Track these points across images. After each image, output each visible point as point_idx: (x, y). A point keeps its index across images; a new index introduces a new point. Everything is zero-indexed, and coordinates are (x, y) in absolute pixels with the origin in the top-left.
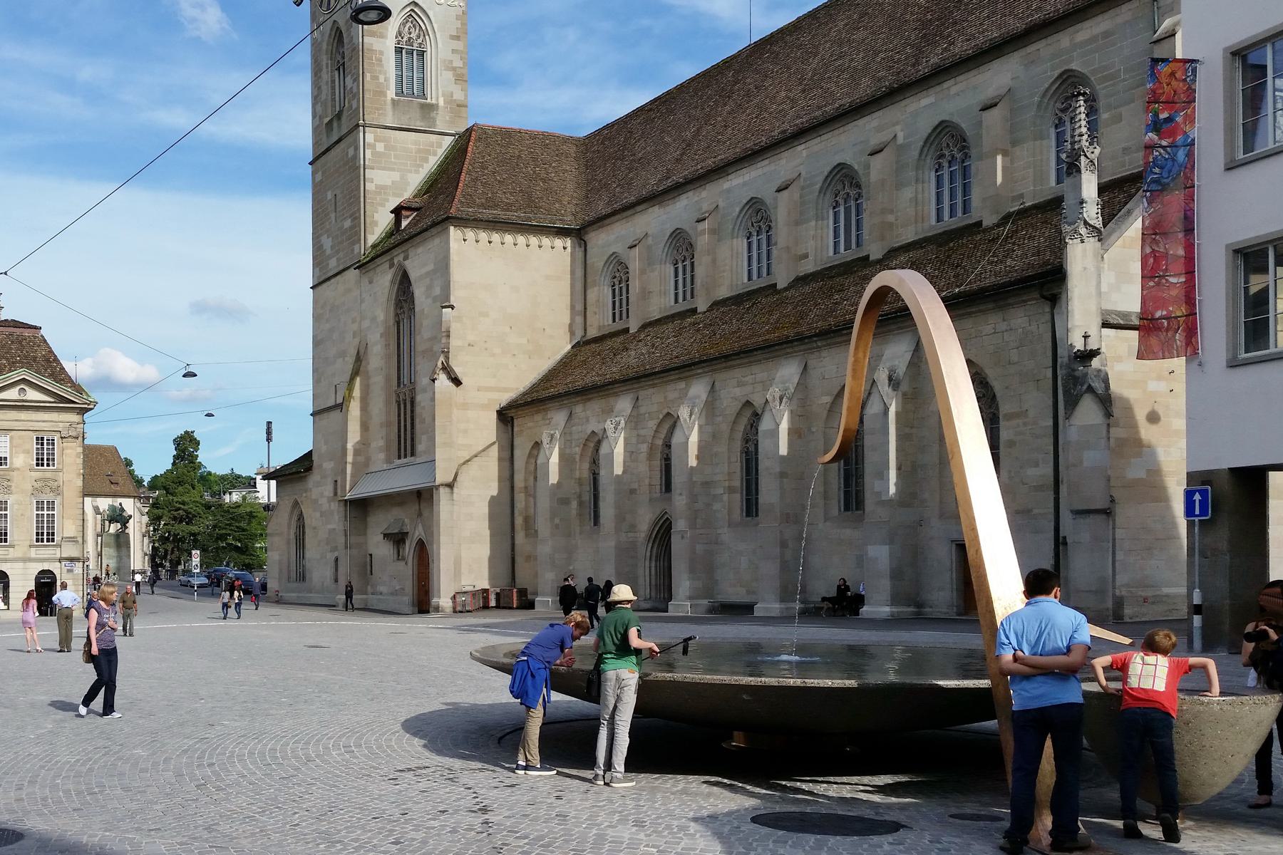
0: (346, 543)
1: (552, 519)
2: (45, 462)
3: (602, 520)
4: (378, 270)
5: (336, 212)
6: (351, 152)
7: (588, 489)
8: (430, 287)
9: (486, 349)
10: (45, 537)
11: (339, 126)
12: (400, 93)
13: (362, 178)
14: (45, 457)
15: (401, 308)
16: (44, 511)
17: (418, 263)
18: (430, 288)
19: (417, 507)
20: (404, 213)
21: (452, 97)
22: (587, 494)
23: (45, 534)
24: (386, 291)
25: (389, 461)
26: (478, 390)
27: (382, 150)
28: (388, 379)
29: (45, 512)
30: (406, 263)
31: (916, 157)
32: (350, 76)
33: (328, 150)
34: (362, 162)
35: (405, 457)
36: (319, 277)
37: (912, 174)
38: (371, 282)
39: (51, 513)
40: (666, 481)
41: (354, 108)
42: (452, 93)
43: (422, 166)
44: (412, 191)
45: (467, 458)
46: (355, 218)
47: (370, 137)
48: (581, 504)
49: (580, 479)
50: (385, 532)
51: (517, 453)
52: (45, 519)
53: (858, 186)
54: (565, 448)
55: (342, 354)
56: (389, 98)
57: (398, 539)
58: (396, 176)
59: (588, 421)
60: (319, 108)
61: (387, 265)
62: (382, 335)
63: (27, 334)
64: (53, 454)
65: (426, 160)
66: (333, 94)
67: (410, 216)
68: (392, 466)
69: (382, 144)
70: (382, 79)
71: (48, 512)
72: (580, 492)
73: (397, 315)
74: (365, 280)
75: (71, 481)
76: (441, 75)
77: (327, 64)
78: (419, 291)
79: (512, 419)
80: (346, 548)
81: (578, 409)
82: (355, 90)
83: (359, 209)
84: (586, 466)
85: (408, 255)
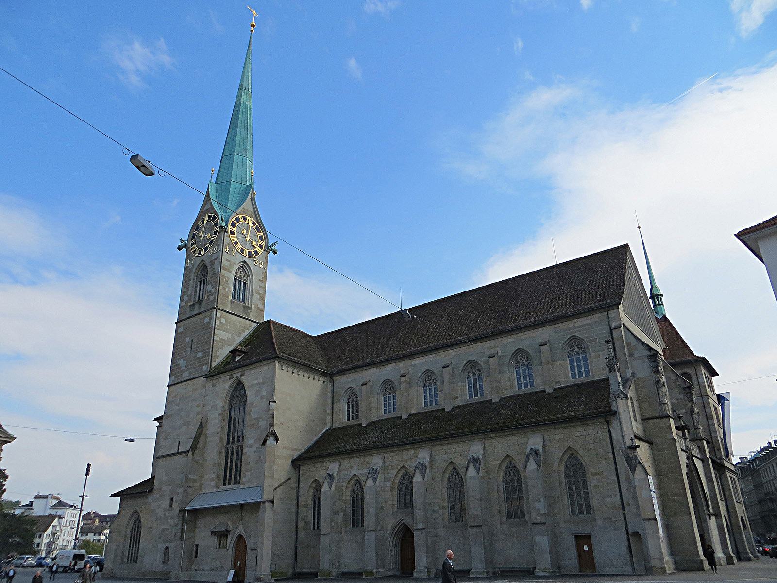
11: (199, 307)
12: (234, 297)
17: (251, 378)
19: (240, 515)
28: (221, 440)
35: (230, 484)
38: (214, 386)
45: (277, 486)
46: (206, 352)
48: (345, 514)
51: (301, 485)
57: (222, 535)
58: (229, 336)
60: (185, 298)
66: (196, 292)
68: (219, 490)
69: (224, 319)
74: (209, 385)
83: (209, 349)
85: (244, 374)
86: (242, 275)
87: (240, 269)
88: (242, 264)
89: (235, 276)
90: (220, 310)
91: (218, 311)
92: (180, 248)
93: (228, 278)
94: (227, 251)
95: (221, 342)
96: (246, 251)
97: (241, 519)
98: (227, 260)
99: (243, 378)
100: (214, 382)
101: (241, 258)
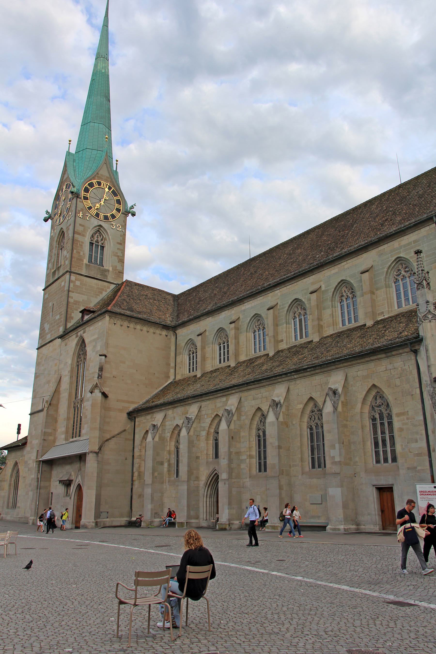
0: (38, 486)
1: (153, 474)
3: (180, 474)
4: (70, 339)
5: (53, 312)
6: (63, 284)
7: (174, 456)
8: (95, 347)
9: (123, 380)
11: (58, 273)
12: (90, 261)
15: (80, 358)
18: (95, 347)
20: (85, 312)
22: (173, 459)
25: (66, 439)
26: (117, 401)
28: (70, 395)
30: (84, 334)
31: (331, 296)
32: (66, 251)
33: (53, 283)
36: (41, 344)
37: (330, 303)
38: (66, 345)
40: (215, 451)
42: (116, 266)
43: (99, 295)
46: (62, 315)
48: (169, 465)
49: (169, 451)
50: (60, 480)
51: (136, 436)
53: (305, 309)
54: (162, 433)
55: (49, 382)
58: (85, 298)
59: (174, 418)
61: (75, 336)
62: (69, 372)
65: (101, 293)
69: (79, 282)
70: (82, 254)
72: (170, 459)
73: (78, 362)
74: (63, 344)
77: (56, 247)
78: (89, 349)
80: (37, 488)
81: (170, 412)
84: (173, 443)
86: (99, 239)
88: (98, 228)
89: (92, 240)
90: (74, 273)
91: (72, 274)
92: (46, 220)
93: (83, 243)
94: (81, 216)
95: (76, 304)
96: (102, 215)
97: (80, 470)
98: (80, 225)
99: (85, 336)
100: (67, 341)
101: (95, 222)
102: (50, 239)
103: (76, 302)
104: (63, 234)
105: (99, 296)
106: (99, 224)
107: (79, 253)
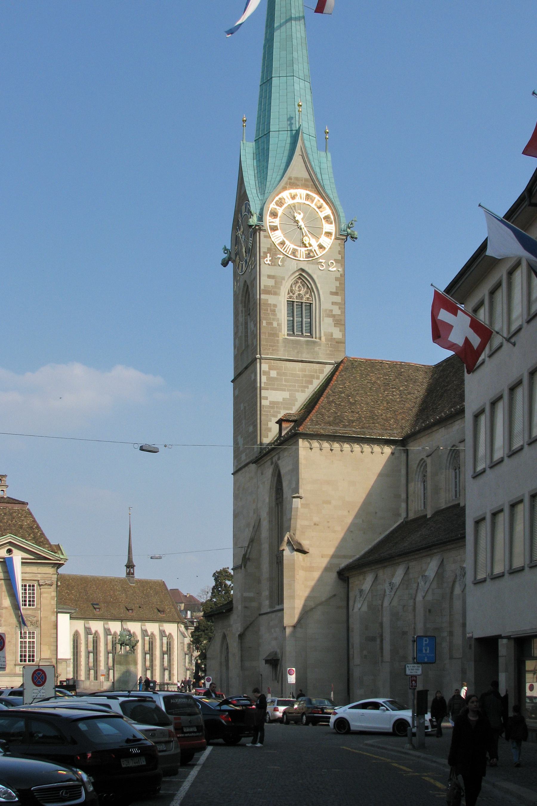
2: (28, 603)
9: (329, 527)
10: (27, 658)
13: (258, 396)
14: (28, 599)
16: (26, 639)
21: (332, 336)
23: (27, 656)
24: (269, 481)
27: (275, 376)
29: (27, 640)
30: (279, 462)
34: (258, 385)
39: (31, 640)
41: (254, 345)
43: (308, 387)
44: (299, 406)
47: (265, 367)
52: (27, 645)
56: (281, 338)
58: (286, 395)
61: (269, 463)
63: (16, 508)
64: (34, 597)
65: (311, 383)
67: (288, 427)
70: (275, 324)
71: (30, 640)
75: (47, 617)
76: (323, 320)
77: (242, 311)
78: (285, 484)
79: (348, 578)
82: (255, 331)
87: (297, 282)
88: (297, 274)
89: (290, 297)
93: (275, 306)
94: (269, 262)
95: (273, 408)
98: (269, 277)
102: (234, 295)
103: (273, 404)
104: (248, 294)
105: (308, 389)
106: (299, 268)
107: (271, 324)
